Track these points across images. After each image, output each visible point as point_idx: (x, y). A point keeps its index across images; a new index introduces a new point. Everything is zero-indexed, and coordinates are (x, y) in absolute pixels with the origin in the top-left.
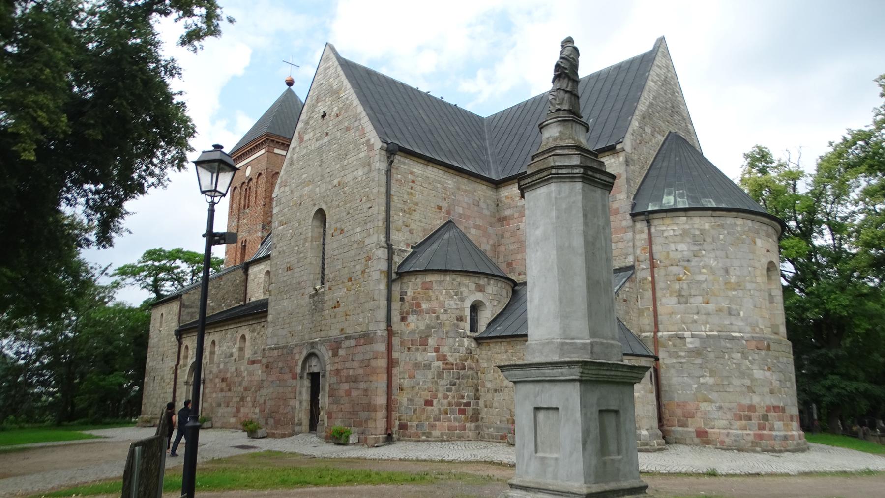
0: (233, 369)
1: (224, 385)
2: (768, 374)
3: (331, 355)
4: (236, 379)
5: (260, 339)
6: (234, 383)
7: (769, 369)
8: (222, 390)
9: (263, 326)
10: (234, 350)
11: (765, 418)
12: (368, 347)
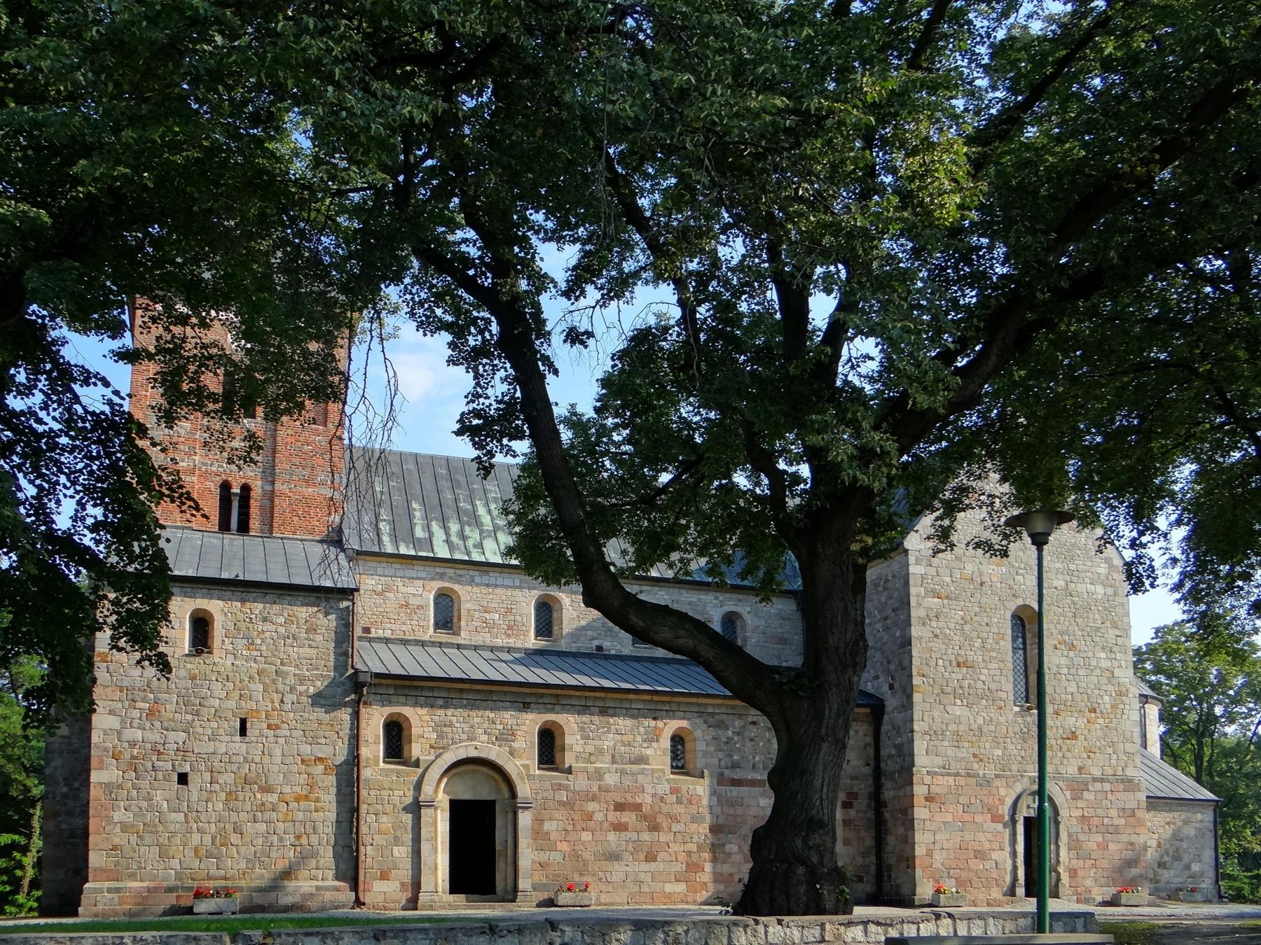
0: (664, 788)
1: (628, 817)
3: (1069, 797)
4: (679, 809)
5: (749, 744)
6: (673, 818)
8: (619, 827)
9: (754, 723)
10: (649, 752)
12: (1130, 795)
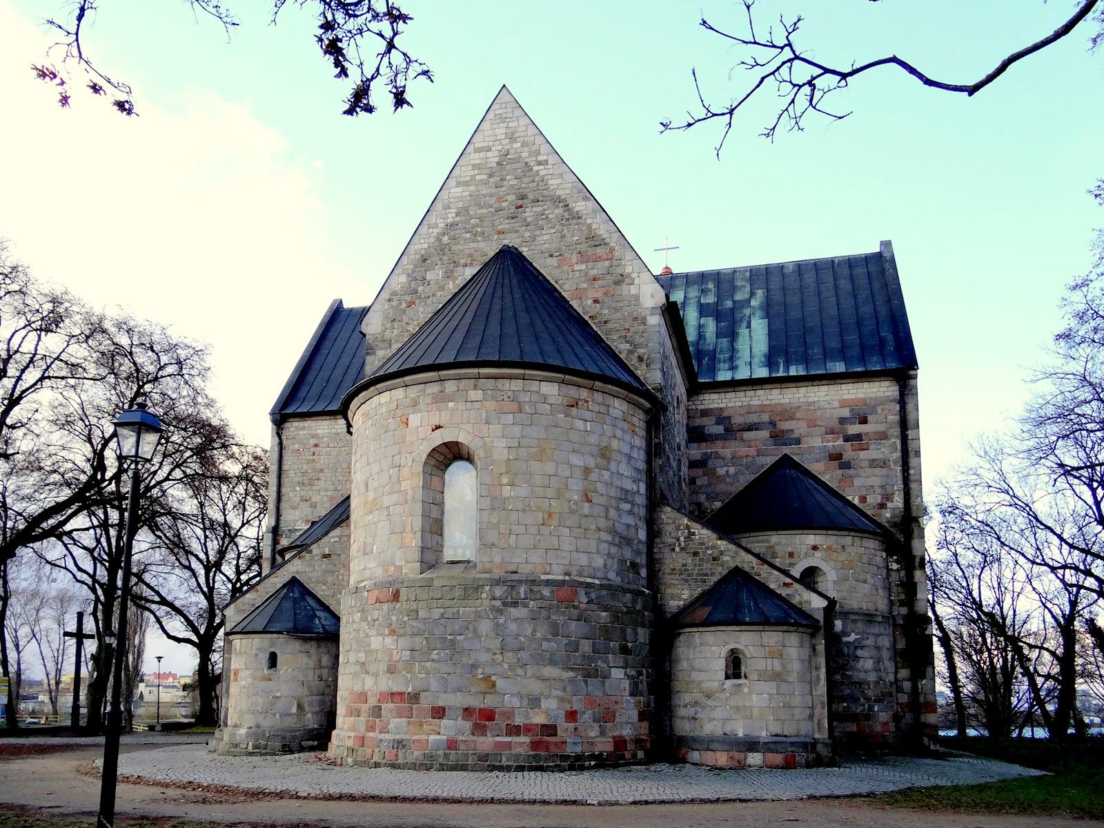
2: (388, 640)
7: (393, 632)
11: (377, 711)
